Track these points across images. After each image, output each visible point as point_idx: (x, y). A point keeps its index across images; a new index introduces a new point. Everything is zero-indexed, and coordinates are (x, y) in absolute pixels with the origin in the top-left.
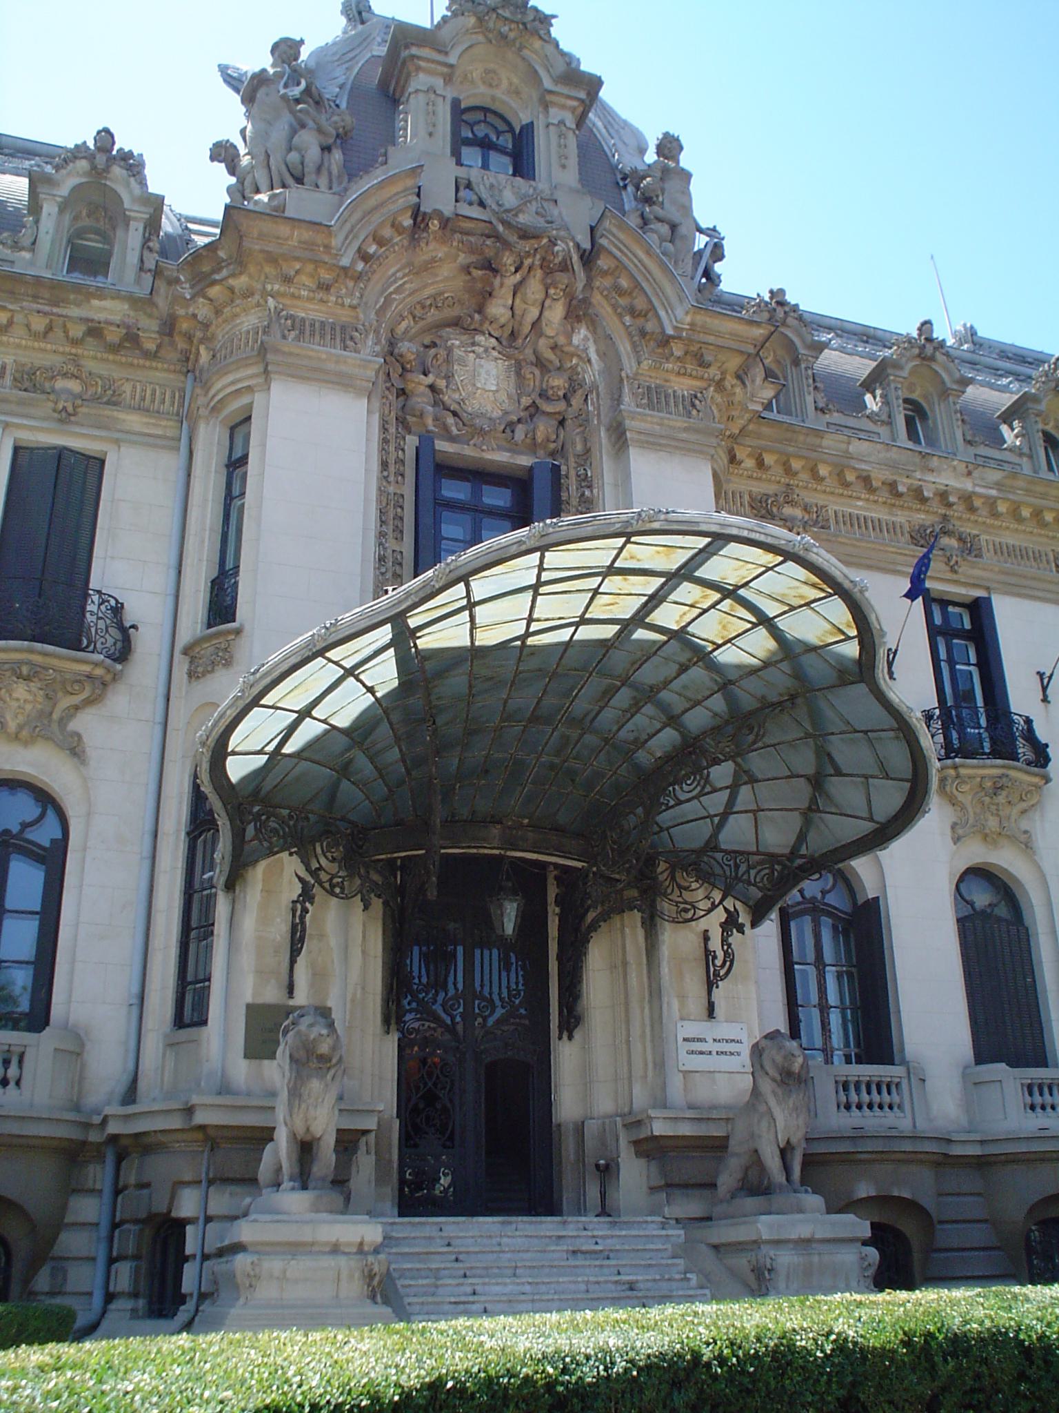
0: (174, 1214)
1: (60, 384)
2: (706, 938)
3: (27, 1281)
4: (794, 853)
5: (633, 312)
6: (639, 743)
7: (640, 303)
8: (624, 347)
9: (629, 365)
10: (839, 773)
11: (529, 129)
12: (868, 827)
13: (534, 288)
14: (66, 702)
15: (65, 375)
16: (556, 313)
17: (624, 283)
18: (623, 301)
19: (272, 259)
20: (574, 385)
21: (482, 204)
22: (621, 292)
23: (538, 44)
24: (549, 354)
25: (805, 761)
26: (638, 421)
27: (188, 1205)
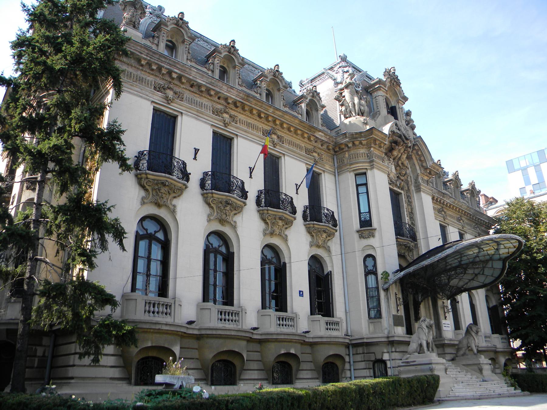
0: (384, 358)
1: (315, 154)
2: (443, 303)
3: (342, 374)
4: (462, 287)
5: (420, 160)
6: (451, 264)
7: (422, 159)
8: (418, 168)
9: (419, 172)
10: (483, 274)
11: (395, 107)
12: (481, 284)
13: (402, 151)
14: (328, 238)
15: (315, 152)
16: (405, 156)
17: (420, 153)
18: (418, 157)
19: (375, 140)
20: (406, 173)
21: (399, 129)
22: (418, 155)
23: (398, 88)
24: (400, 165)
25: (476, 271)
26: (423, 186)
27: (386, 357)
